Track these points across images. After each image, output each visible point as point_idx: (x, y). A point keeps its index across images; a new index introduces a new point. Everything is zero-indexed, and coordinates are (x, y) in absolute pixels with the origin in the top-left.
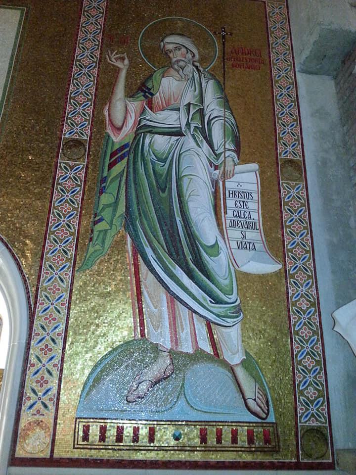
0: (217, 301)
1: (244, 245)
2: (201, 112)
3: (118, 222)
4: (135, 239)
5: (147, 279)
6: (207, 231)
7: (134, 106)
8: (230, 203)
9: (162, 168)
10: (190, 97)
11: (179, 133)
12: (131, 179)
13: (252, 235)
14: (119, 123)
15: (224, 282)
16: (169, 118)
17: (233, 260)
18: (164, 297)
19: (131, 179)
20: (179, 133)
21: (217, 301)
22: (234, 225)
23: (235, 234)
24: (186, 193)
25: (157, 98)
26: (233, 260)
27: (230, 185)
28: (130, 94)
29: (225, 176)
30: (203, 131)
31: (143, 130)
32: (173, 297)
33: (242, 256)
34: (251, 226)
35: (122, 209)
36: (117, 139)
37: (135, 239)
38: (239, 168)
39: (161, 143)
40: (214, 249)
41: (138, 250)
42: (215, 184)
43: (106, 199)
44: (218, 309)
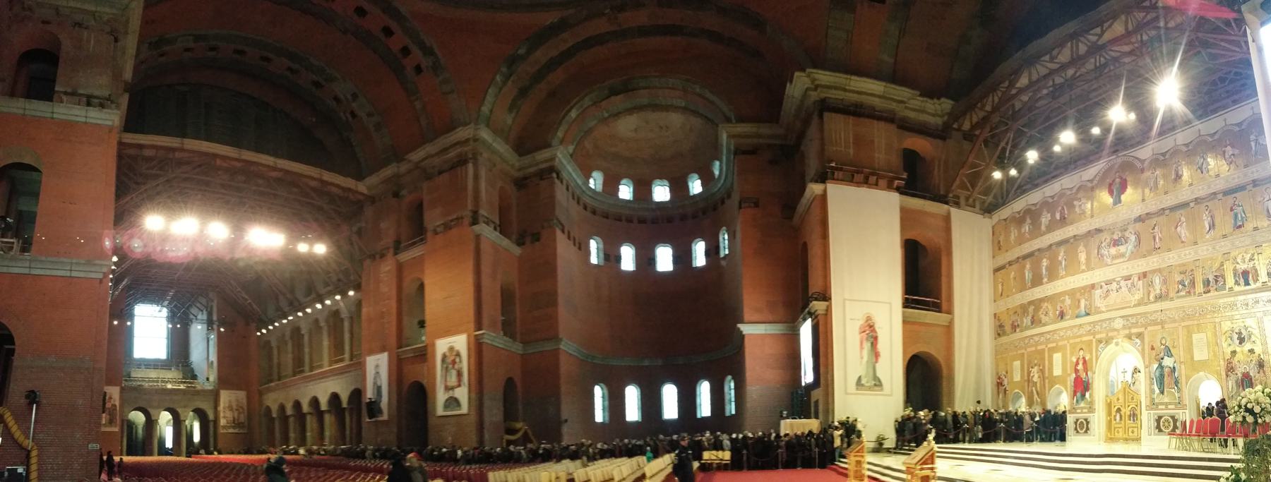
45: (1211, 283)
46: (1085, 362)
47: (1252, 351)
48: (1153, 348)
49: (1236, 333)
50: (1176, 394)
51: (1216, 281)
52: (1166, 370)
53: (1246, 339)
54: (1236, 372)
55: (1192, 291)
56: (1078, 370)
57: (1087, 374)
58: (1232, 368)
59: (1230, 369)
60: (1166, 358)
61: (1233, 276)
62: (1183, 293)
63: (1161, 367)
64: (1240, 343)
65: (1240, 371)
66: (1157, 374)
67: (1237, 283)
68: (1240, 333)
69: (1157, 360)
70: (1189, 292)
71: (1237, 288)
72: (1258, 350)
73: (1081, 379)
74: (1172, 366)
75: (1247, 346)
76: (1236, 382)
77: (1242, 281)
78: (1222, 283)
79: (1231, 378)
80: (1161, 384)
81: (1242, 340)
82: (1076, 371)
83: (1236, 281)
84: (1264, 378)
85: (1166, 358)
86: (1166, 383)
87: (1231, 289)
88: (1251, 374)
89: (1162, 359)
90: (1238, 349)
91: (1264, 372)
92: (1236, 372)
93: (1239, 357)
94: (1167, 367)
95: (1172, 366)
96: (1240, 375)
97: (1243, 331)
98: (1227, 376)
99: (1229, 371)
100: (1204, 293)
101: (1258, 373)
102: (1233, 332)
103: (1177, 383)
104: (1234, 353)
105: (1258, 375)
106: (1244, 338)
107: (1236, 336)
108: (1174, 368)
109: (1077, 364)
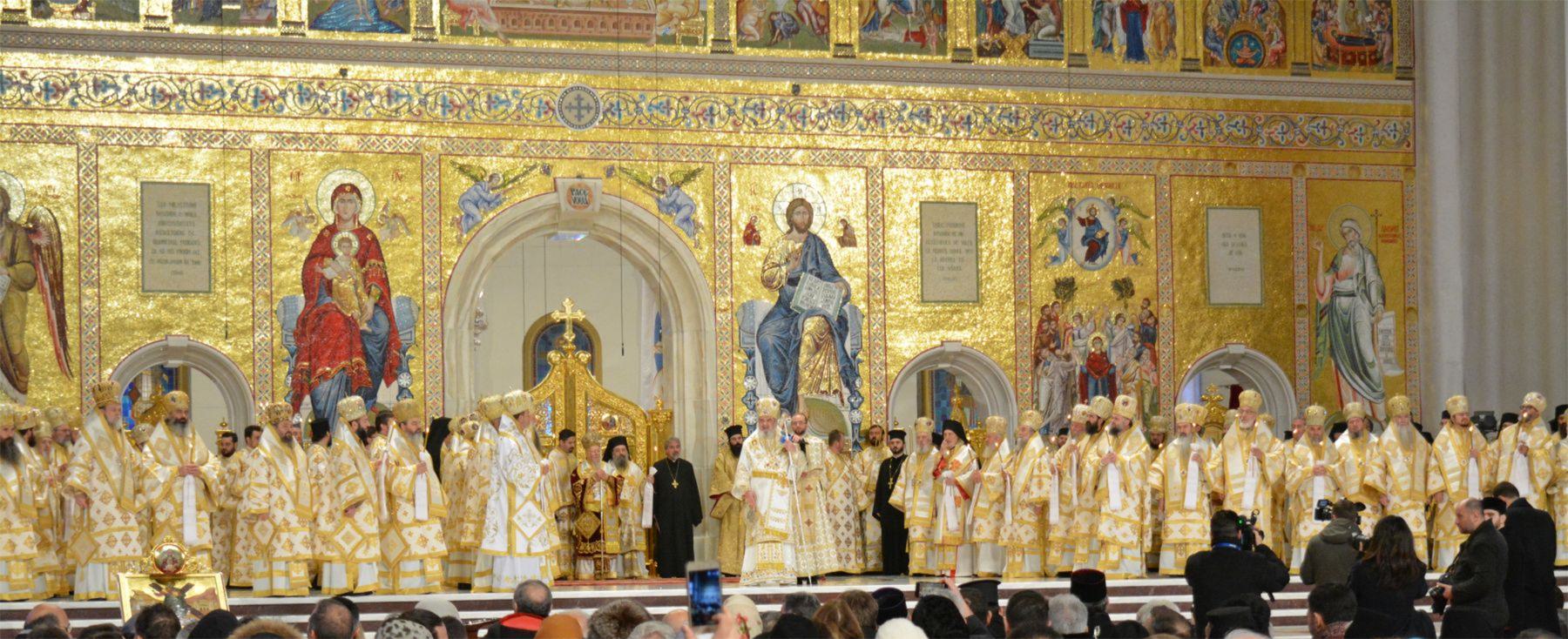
0: (1374, 391)
1: (1387, 361)
2: (1365, 278)
3: (1327, 352)
4: (1336, 361)
5: (1343, 382)
6: (1369, 355)
7: (1329, 278)
8: (1380, 337)
9: (1346, 318)
10: (1358, 270)
11: (1352, 295)
12: (1331, 325)
13: (1391, 355)
14: (1322, 290)
15: (1376, 380)
16: (1347, 285)
17: (1381, 368)
18: (1350, 391)
19: (1331, 325)
20: (1352, 295)
21: (1374, 391)
22: (1382, 349)
23: (1382, 355)
24: (1359, 332)
25: (1341, 271)
26: (1382, 371)
27: (1381, 326)
28: (1327, 271)
29: (1378, 320)
30: (1365, 291)
31: (1336, 294)
32: (1354, 390)
33: (1386, 367)
34: (1390, 350)
35: (1328, 345)
36: (1323, 301)
37: (1336, 361)
38: (1386, 314)
39: (1344, 302)
40: (1372, 364)
41: (1337, 367)
42: (1372, 325)
43: (1321, 339)
44: (1375, 395)
45: (1009, 20)
46: (370, 249)
47: (1123, 288)
48: (751, 237)
49: (1082, 222)
50: (846, 414)
51: (1031, 17)
52: (810, 325)
53: (1111, 245)
54: (1068, 349)
55: (932, 34)
56: (329, 286)
57: (383, 304)
58: (1055, 337)
59: (1048, 338)
60: (808, 280)
61: (1090, 15)
62: (895, 35)
63: (785, 310)
64: (1091, 256)
65: (1078, 350)
66: (770, 339)
67: (1102, 42)
68: (1091, 223)
69: (767, 283)
70: (920, 36)
71: (1098, 62)
72: (1143, 284)
73: (350, 322)
74: (832, 311)
75: (1115, 265)
76: (1066, 382)
77: (1119, 38)
78: (1051, 28)
79: (1050, 370)
80: (784, 374)
81: (1095, 249)
82: (314, 283)
83: (1101, 33)
84: (1153, 375)
85: (808, 280)
86: (805, 375)
87: (1078, 60)
88: (1113, 360)
89: (793, 281)
90: (1082, 278)
91: (1155, 359)
92: (1068, 349)
93: (1081, 302)
94: (812, 313)
95: (832, 311)
96: (1079, 362)
97: (1107, 222)
98: (1037, 361)
99: (1044, 345)
100: (982, 52)
101: (1138, 358)
102: (1070, 213)
103: (849, 373)
104: (1066, 287)
105: (1133, 366)
106: (1104, 240)
107: (1079, 231)
108: (842, 320)
109: (321, 250)
